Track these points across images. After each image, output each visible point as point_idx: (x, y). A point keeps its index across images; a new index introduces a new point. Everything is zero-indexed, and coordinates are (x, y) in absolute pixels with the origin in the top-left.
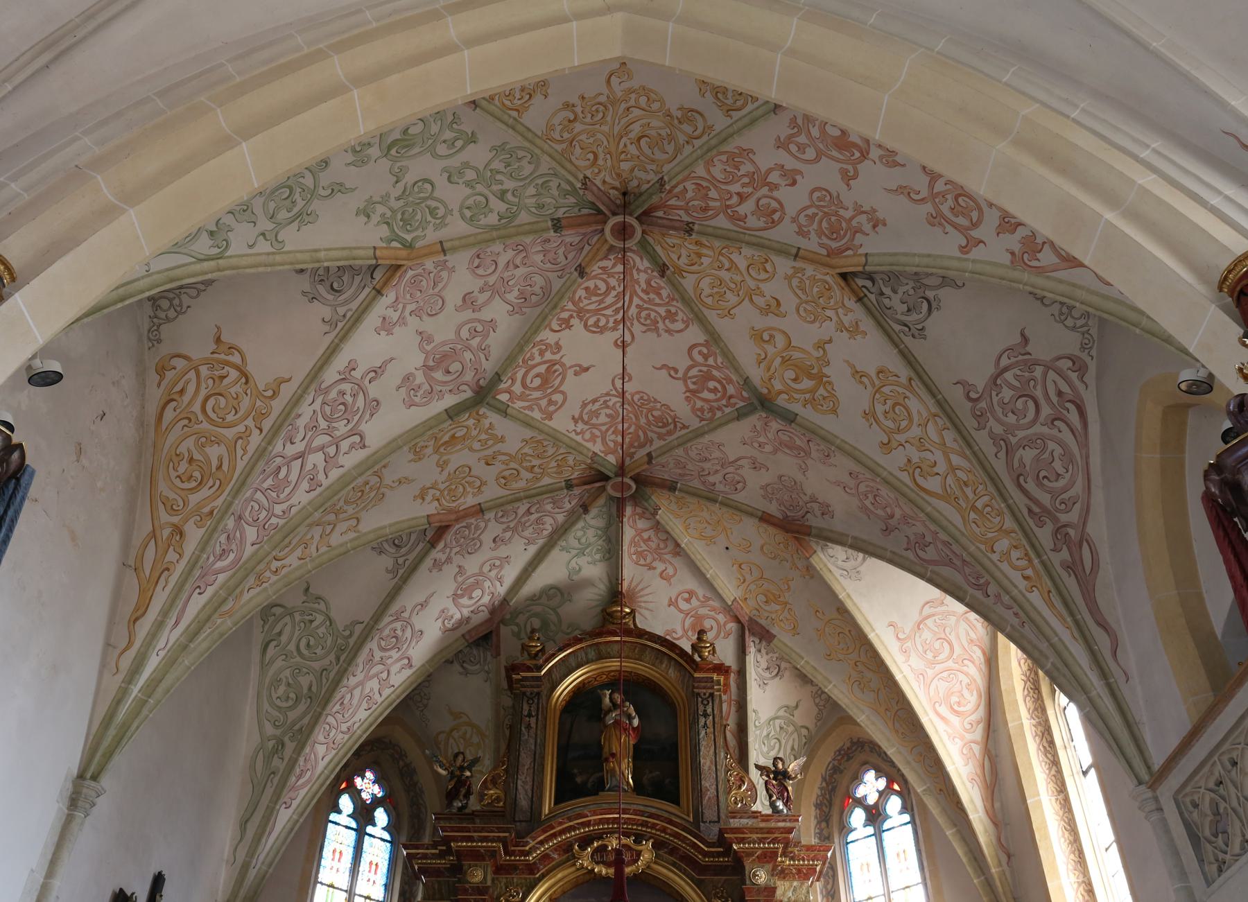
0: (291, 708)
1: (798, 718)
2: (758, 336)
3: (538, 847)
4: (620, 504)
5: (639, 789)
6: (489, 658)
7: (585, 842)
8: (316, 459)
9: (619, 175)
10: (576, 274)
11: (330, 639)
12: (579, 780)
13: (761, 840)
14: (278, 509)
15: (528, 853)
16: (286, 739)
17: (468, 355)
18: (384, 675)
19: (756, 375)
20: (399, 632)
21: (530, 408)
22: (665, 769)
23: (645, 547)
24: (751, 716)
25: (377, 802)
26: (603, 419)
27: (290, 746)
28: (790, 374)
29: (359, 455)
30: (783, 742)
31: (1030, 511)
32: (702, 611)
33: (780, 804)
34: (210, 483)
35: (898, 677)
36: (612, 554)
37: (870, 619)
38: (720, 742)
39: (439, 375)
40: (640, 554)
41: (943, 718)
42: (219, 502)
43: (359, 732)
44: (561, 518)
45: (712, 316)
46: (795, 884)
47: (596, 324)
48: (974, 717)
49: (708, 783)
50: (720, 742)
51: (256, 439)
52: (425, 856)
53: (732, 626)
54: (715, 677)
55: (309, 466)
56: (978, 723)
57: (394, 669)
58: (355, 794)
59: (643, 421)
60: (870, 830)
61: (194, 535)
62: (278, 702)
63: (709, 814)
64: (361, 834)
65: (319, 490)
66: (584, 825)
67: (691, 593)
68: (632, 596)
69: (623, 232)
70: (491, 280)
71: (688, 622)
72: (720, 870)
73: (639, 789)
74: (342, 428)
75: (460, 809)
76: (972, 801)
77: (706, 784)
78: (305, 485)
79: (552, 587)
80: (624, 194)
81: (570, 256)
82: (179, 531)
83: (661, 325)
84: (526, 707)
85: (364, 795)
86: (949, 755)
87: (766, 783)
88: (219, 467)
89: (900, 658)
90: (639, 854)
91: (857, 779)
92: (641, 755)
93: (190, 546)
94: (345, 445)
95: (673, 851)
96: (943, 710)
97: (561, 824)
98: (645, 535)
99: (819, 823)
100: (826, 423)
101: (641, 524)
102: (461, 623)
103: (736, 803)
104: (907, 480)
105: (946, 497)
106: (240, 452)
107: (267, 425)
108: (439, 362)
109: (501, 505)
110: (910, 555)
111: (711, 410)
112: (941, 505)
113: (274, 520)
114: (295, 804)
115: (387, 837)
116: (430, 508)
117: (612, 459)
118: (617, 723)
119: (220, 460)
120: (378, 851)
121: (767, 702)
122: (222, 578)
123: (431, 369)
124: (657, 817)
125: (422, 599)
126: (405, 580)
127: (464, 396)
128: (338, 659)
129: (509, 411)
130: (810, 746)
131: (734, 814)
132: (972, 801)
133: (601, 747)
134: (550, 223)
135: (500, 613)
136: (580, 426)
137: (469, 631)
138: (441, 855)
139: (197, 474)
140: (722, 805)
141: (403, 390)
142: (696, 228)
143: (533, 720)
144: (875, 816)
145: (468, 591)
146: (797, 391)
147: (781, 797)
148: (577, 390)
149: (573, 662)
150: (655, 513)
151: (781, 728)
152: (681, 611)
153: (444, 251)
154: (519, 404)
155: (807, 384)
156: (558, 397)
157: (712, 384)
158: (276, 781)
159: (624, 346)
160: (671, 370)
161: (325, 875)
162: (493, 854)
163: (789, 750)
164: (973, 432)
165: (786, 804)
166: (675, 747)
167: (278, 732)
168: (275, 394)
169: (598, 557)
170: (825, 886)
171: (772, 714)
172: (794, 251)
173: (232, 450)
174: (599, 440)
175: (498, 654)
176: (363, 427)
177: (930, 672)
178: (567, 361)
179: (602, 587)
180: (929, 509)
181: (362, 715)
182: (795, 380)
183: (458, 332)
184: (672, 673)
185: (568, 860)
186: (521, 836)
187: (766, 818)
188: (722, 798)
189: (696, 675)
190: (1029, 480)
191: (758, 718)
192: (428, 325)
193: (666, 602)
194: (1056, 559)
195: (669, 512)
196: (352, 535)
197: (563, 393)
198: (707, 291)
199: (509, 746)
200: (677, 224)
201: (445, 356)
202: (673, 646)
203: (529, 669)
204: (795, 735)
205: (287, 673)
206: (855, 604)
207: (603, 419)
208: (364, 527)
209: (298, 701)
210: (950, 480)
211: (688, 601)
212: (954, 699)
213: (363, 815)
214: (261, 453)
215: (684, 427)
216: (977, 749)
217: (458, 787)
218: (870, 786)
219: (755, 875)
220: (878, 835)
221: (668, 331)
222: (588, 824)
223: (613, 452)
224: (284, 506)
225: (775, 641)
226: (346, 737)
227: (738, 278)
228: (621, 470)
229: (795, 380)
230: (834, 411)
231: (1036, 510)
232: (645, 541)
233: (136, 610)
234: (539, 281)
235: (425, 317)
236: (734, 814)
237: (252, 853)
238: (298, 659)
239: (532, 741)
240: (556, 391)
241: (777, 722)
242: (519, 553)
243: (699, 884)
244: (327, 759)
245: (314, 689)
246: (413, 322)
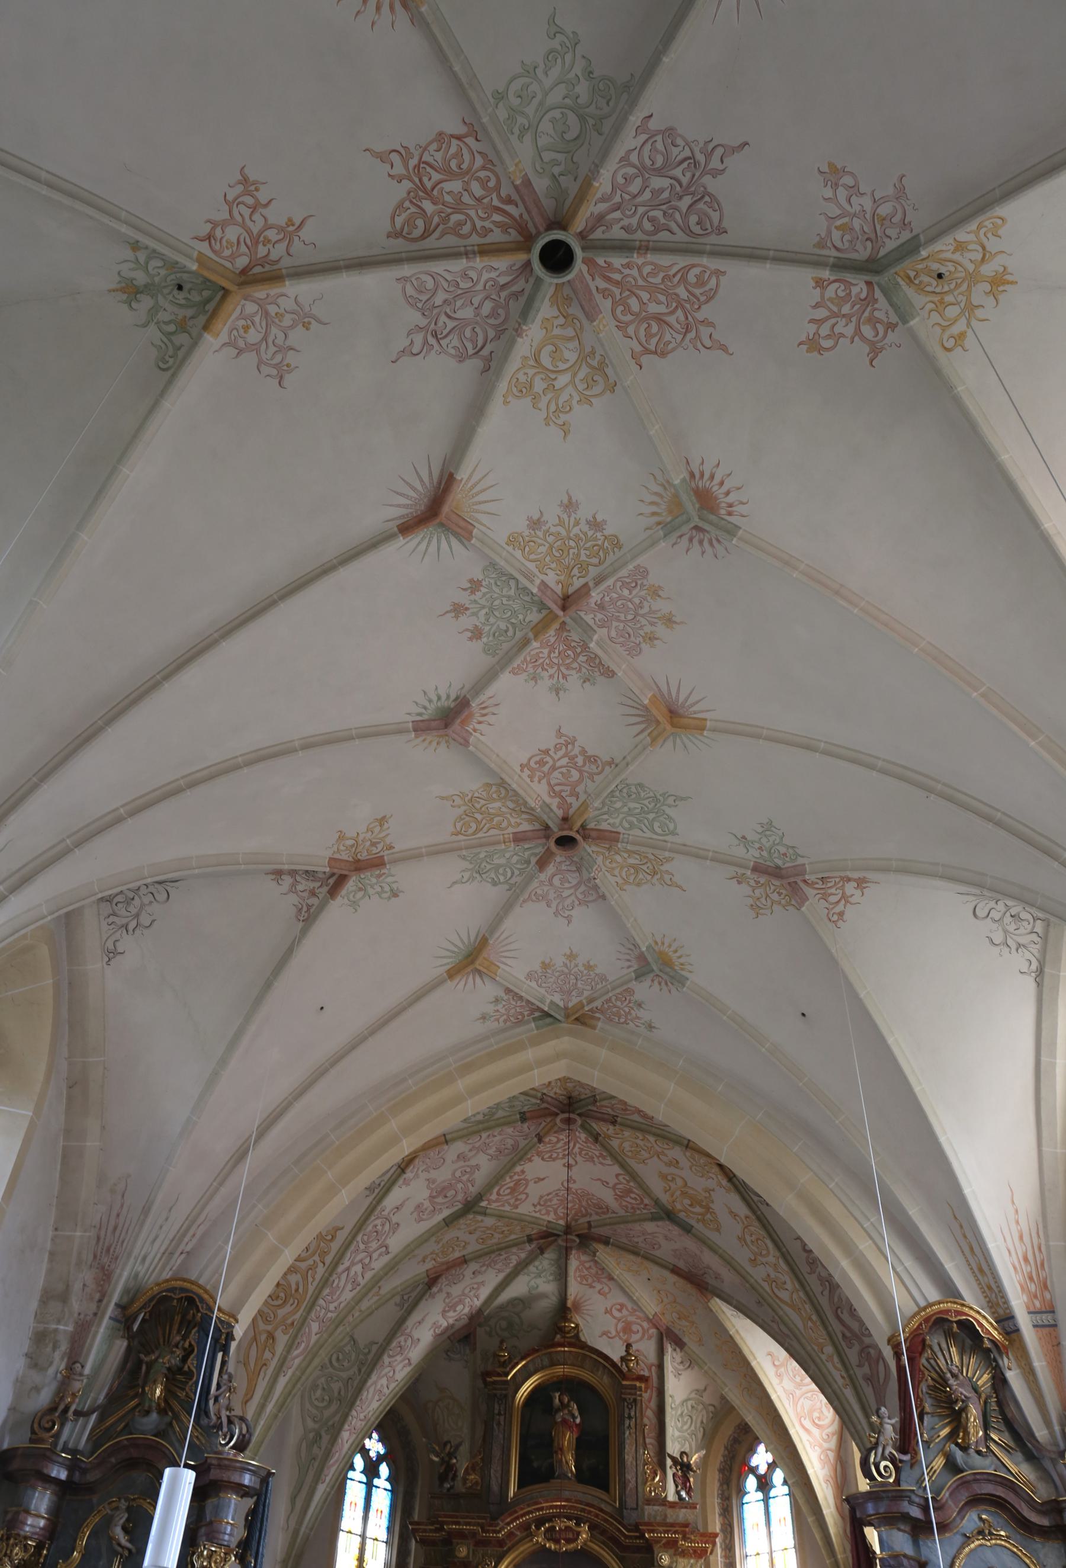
0: (326, 1407)
1: (707, 1398)
2: (664, 1177)
3: (506, 1528)
4: (567, 1250)
5: (581, 1477)
6: (468, 1351)
7: (540, 1522)
8: (358, 1268)
9: (565, 1089)
10: (536, 1140)
11: (354, 1354)
12: (535, 1464)
13: (667, 1532)
14: (332, 1307)
15: (499, 1532)
16: (323, 1434)
17: (460, 1186)
18: (391, 1374)
19: (664, 1198)
20: (403, 1343)
21: (503, 1205)
22: (599, 1465)
23: (586, 1272)
24: (668, 1400)
25: (381, 1458)
26: (555, 1201)
27: (326, 1438)
28: (687, 1202)
29: (386, 1259)
30: (694, 1418)
31: (844, 1335)
32: (631, 1319)
33: (683, 1494)
34: (291, 1301)
35: (773, 1397)
36: (562, 1276)
37: (754, 1351)
38: (640, 1440)
39: (440, 1200)
40: (583, 1277)
41: (806, 1430)
42: (297, 1316)
43: (373, 1419)
44: (523, 1255)
45: (632, 1163)
46: (692, 1561)
47: (550, 1157)
48: (830, 1430)
49: (630, 1476)
50: (640, 1440)
51: (321, 1270)
52: (425, 1531)
53: (653, 1331)
54: (638, 1384)
55: (352, 1273)
56: (833, 1434)
57: (398, 1368)
58: (365, 1452)
59: (584, 1203)
60: (760, 1495)
61: (282, 1339)
62: (316, 1403)
63: (630, 1502)
64: (369, 1486)
65: (358, 1288)
66: (539, 1510)
67: (622, 1306)
68: (577, 1306)
69: (569, 1121)
70: (477, 1145)
71: (620, 1326)
72: (638, 1549)
73: (581, 1477)
74: (374, 1245)
75: (449, 1490)
76: (826, 1499)
77: (628, 1477)
78: (349, 1287)
79: (516, 1299)
80: (570, 1098)
81: (532, 1128)
82: (271, 1336)
83: (596, 1159)
84: (496, 1406)
85: (373, 1454)
86: (810, 1461)
87: (674, 1475)
88: (297, 1290)
89: (775, 1381)
90: (578, 1534)
91: (752, 1450)
92: (581, 1447)
93: (280, 1348)
94: (375, 1256)
95: (603, 1532)
96: (807, 1423)
97: (522, 1509)
98: (587, 1265)
99: (721, 1485)
100: (713, 1236)
101: (584, 1258)
102: (447, 1329)
103: (650, 1492)
104: (767, 1288)
105: (792, 1306)
106: (310, 1279)
107: (328, 1259)
108: (439, 1193)
109: (478, 1256)
110: (775, 1326)
111: (633, 1208)
112: (790, 1311)
113: (330, 1315)
114: (328, 1479)
115: (389, 1487)
116: (429, 1265)
117: (562, 1222)
118: (565, 1421)
119: (297, 1284)
120: (382, 1499)
121: (679, 1387)
122: (297, 1361)
123: (434, 1197)
124: (592, 1506)
125: (419, 1318)
126: (409, 1312)
127: (456, 1208)
128: (360, 1371)
129: (488, 1211)
130: (708, 1439)
131: (649, 1501)
132: (826, 1499)
133: (552, 1441)
134: (518, 1116)
135: (477, 1318)
136: (538, 1207)
137: (453, 1334)
138: (437, 1530)
139: (282, 1295)
140: (640, 1495)
141: (415, 1214)
142: (619, 1119)
143: (502, 1418)
144: (764, 1484)
145: (453, 1308)
146: (693, 1213)
147: (684, 1487)
148: (534, 1191)
149: (531, 1368)
150: (595, 1255)
151: (693, 1407)
152: (614, 1317)
153: (447, 1142)
154: (494, 1205)
155: (698, 1209)
156: (523, 1196)
157: (633, 1195)
158: (316, 1464)
159: (569, 1166)
160: (605, 1183)
161: (345, 1524)
162: (474, 1534)
163: (699, 1424)
164: (806, 1276)
165: (688, 1493)
166: (606, 1438)
167: (316, 1426)
168: (333, 1237)
169: (551, 1278)
170: (724, 1541)
171: (684, 1397)
172: (686, 1142)
173: (305, 1278)
174: (552, 1214)
175: (475, 1349)
176: (389, 1242)
177: (798, 1392)
178: (529, 1178)
179: (554, 1298)
180: (781, 1313)
181: (375, 1405)
182: (691, 1205)
183: (453, 1174)
184: (606, 1379)
185: (527, 1536)
186: (494, 1518)
187: (673, 1505)
188: (640, 1489)
189: (624, 1383)
190: (845, 1312)
191: (674, 1401)
192: (433, 1174)
193: (603, 1310)
194: (859, 1373)
195: (604, 1254)
196: (376, 1298)
197: (527, 1194)
198: (628, 1149)
199: (484, 1440)
200: (606, 1116)
201: (444, 1189)
202: (606, 1358)
203: (499, 1375)
204: (704, 1412)
205: (323, 1380)
206: (742, 1338)
207: (555, 1201)
208: (382, 1292)
209: (330, 1401)
210: (795, 1296)
211: (620, 1310)
212: (816, 1414)
213: (371, 1471)
214: (325, 1282)
215: (614, 1212)
216: (831, 1455)
217: (448, 1472)
218: (761, 1458)
219: (661, 1558)
220: (766, 1500)
221: (601, 1163)
222: (542, 1509)
223: (561, 1218)
224: (335, 1304)
225: (686, 1348)
226: (363, 1423)
227: (649, 1145)
228: (568, 1229)
229: (691, 1205)
230: (718, 1230)
231: (848, 1334)
232: (587, 1269)
233: (246, 1395)
234: (510, 1142)
235: (432, 1171)
236: (649, 1501)
237: (300, 1523)
238: (331, 1370)
239: (501, 1436)
240: (522, 1193)
241: (690, 1403)
242: (492, 1279)
243: (622, 1560)
244: (350, 1442)
245: (342, 1393)
246: (424, 1176)
